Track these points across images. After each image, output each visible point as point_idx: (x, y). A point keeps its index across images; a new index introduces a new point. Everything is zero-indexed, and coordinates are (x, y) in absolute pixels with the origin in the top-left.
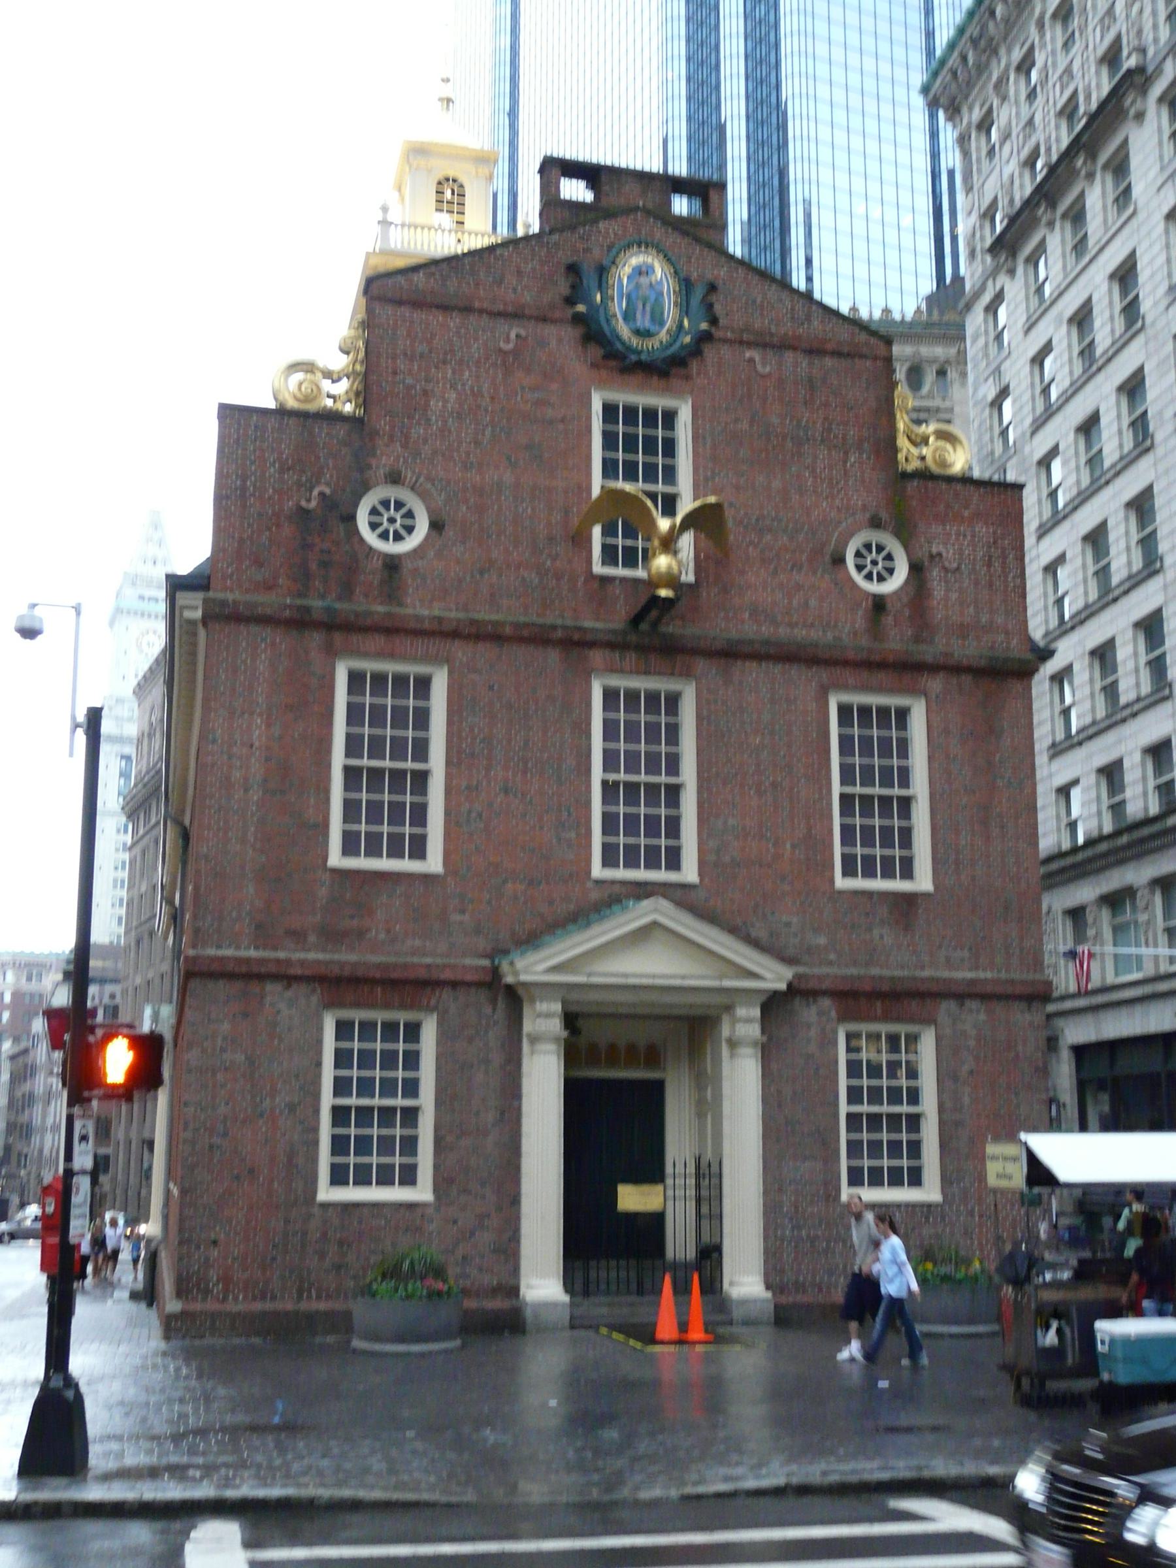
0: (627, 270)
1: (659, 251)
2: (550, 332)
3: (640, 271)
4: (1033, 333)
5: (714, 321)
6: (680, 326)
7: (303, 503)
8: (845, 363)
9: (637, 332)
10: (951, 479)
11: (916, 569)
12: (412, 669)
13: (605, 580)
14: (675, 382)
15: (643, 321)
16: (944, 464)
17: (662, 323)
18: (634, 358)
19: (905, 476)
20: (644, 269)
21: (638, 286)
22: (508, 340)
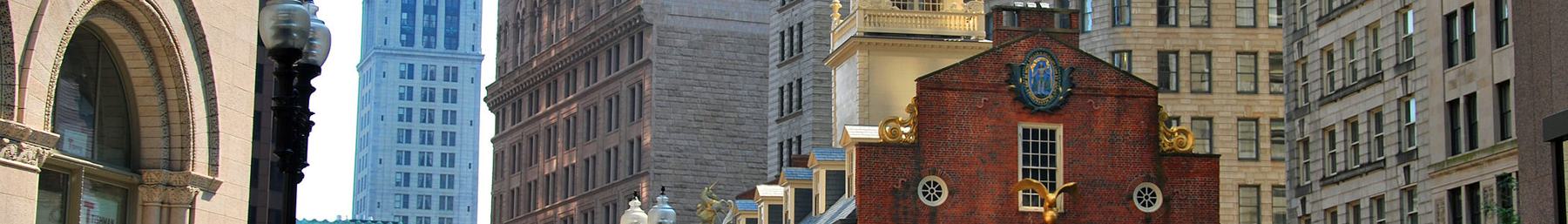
1: (1049, 54)
3: (1038, 66)
6: (1058, 91)
7: (895, 186)
9: (1038, 96)
11: (1165, 201)
13: (1024, 213)
14: (1054, 117)
15: (1041, 90)
16: (1181, 145)
17: (1049, 91)
18: (1037, 108)
19: (1164, 154)
20: (1041, 64)
21: (1039, 74)
22: (980, 104)
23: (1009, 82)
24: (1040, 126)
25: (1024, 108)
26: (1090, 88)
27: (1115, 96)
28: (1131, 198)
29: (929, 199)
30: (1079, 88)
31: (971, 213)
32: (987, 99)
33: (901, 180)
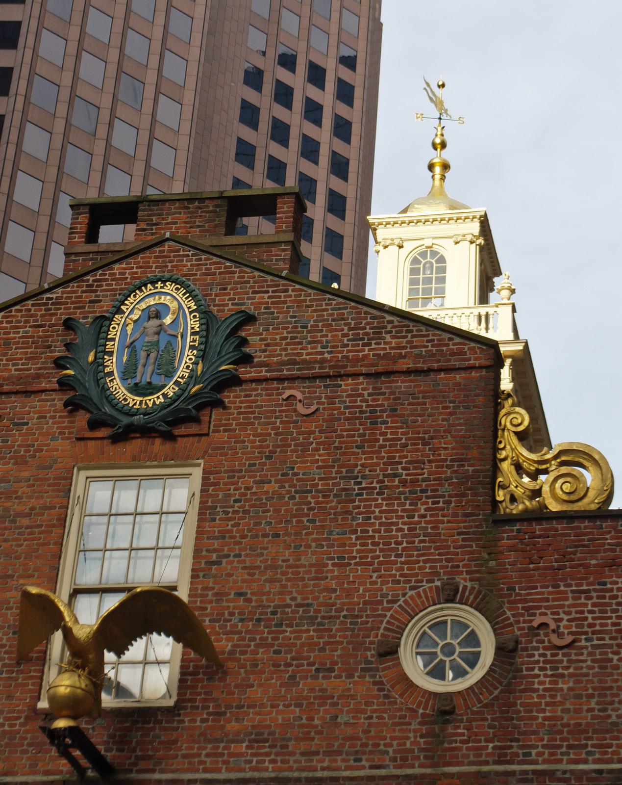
5: (246, 359)
8: (423, 382)
15: (145, 375)
17: (169, 375)
18: (125, 420)
26: (293, 363)
27: (368, 375)
30: (261, 364)
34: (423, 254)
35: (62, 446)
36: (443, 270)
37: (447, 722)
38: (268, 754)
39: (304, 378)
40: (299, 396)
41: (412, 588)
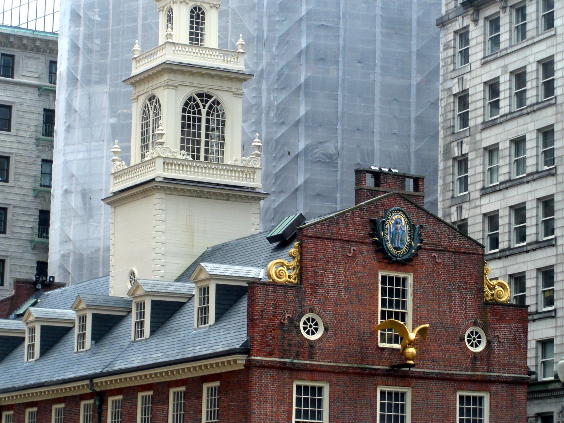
0: (393, 222)
1: (404, 213)
2: (364, 247)
4: (487, 68)
7: (282, 321)
8: (467, 257)
9: (395, 248)
10: (502, 304)
11: (489, 342)
12: (317, 384)
13: (383, 349)
17: (403, 244)
18: (394, 259)
19: (487, 303)
20: (399, 220)
22: (350, 252)
23: (372, 236)
24: (395, 274)
25: (384, 258)
27: (453, 252)
28: (463, 340)
29: (308, 333)
30: (427, 244)
31: (342, 347)
32: (355, 249)
33: (287, 315)
34: (195, 8)
35: (374, 262)
36: (203, 19)
37: (476, 360)
38: (435, 365)
39: (436, 250)
40: (437, 257)
41: (467, 321)
